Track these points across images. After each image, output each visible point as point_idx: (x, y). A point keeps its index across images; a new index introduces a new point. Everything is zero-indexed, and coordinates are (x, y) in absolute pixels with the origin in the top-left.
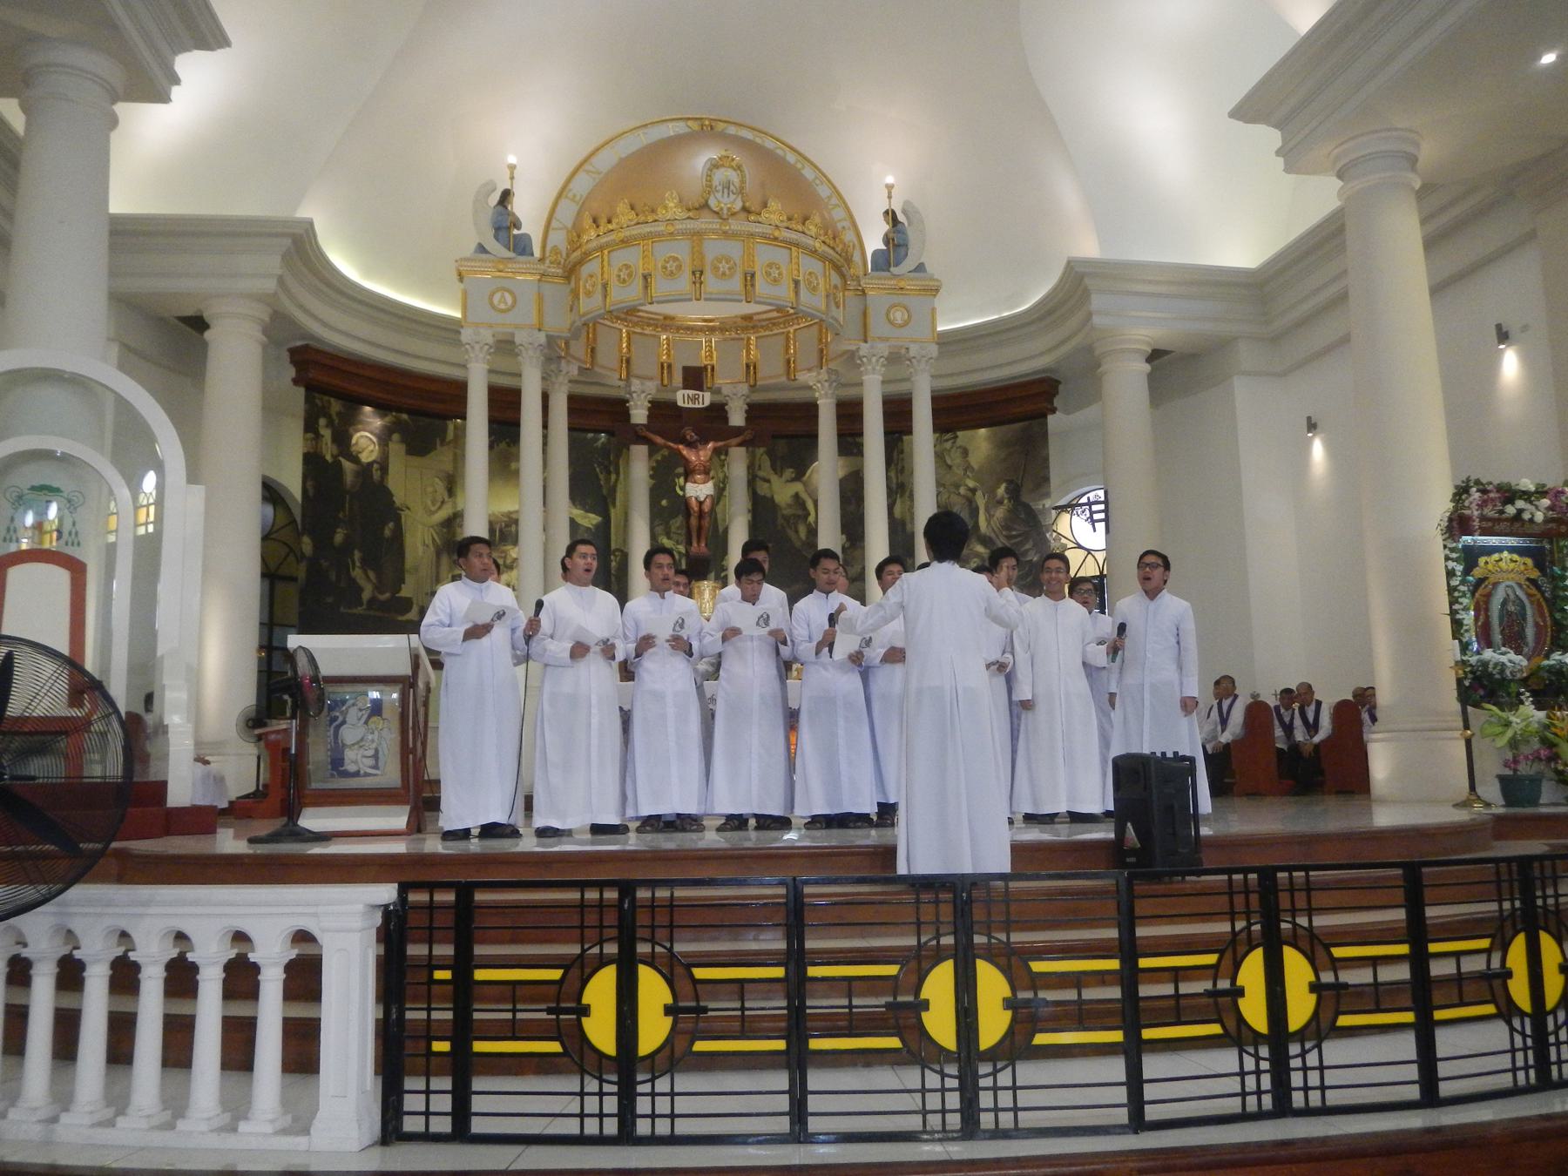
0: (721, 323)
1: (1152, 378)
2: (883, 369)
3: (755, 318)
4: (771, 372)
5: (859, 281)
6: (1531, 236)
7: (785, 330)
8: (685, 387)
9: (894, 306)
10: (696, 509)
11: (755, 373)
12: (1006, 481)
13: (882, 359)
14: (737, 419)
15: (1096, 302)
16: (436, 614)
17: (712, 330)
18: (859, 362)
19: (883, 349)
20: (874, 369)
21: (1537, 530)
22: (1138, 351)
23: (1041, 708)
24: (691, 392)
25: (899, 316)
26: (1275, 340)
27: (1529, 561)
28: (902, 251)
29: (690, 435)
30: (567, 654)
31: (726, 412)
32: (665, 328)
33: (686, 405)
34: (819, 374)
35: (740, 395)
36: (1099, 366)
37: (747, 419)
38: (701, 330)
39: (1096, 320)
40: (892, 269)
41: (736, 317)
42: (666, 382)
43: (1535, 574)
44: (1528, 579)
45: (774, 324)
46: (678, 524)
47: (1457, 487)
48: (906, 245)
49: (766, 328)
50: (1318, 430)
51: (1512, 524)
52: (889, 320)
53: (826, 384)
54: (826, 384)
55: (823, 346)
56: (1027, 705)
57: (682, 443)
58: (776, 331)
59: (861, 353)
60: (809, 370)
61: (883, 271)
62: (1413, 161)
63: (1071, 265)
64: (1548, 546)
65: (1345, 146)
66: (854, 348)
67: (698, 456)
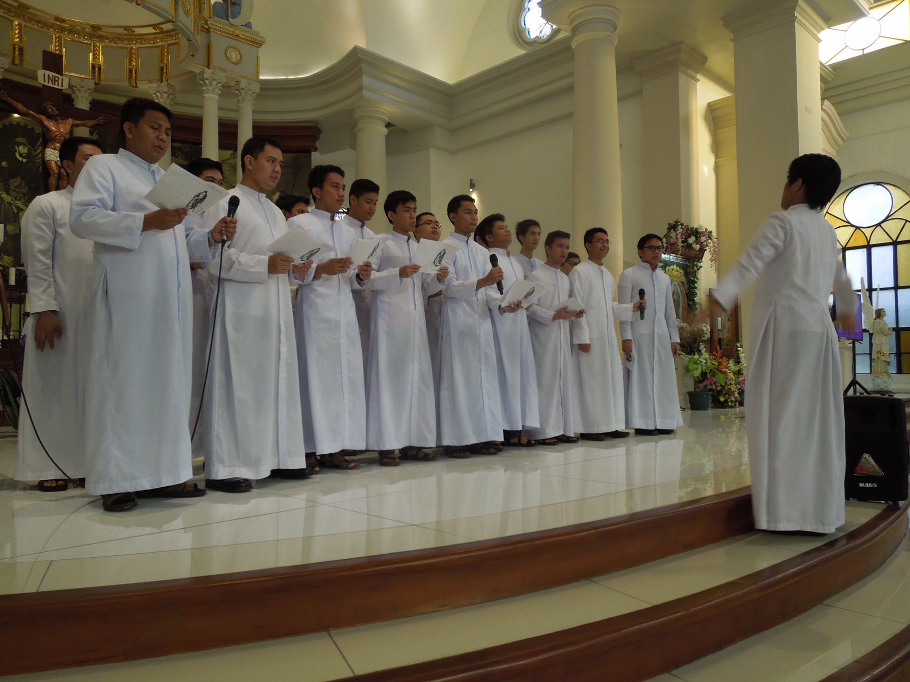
0: (70, 25)
1: (388, 137)
2: (220, 92)
3: (103, 28)
4: (115, 78)
5: (207, 21)
6: (638, 93)
7: (128, 46)
8: (44, 68)
9: (228, 47)
10: (56, 171)
11: (99, 74)
12: (280, 191)
13: (220, 85)
14: (82, 103)
15: (366, 81)
16: (93, 187)
17: (63, 29)
18: (201, 82)
19: (222, 77)
20: (214, 90)
21: (692, 254)
22: (383, 120)
23: (595, 350)
24: (52, 74)
25: (234, 56)
26: (453, 131)
27: (682, 271)
28: (237, 7)
29: (51, 109)
30: (264, 268)
31: (73, 100)
32: (17, 16)
33: (46, 84)
34: (160, 86)
35: (86, 88)
36: (356, 125)
37: (90, 108)
38: (52, 26)
39: (365, 93)
40: (230, 19)
41: (87, 24)
42: (17, 62)
43: (684, 279)
44: (681, 282)
45: (119, 39)
46: (16, 184)
47: (669, 224)
48: (239, 5)
49: (112, 40)
50: (475, 188)
51: (686, 250)
52: (227, 57)
53: (165, 95)
54: (165, 95)
55: (163, 65)
56: (584, 348)
57: (43, 115)
58: (121, 45)
59: (205, 76)
60: (150, 82)
61: (222, 18)
62: (615, 28)
63: (356, 50)
64: (689, 264)
65: (588, 9)
66: (197, 71)
67: (59, 128)
